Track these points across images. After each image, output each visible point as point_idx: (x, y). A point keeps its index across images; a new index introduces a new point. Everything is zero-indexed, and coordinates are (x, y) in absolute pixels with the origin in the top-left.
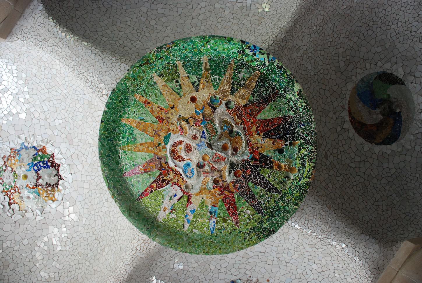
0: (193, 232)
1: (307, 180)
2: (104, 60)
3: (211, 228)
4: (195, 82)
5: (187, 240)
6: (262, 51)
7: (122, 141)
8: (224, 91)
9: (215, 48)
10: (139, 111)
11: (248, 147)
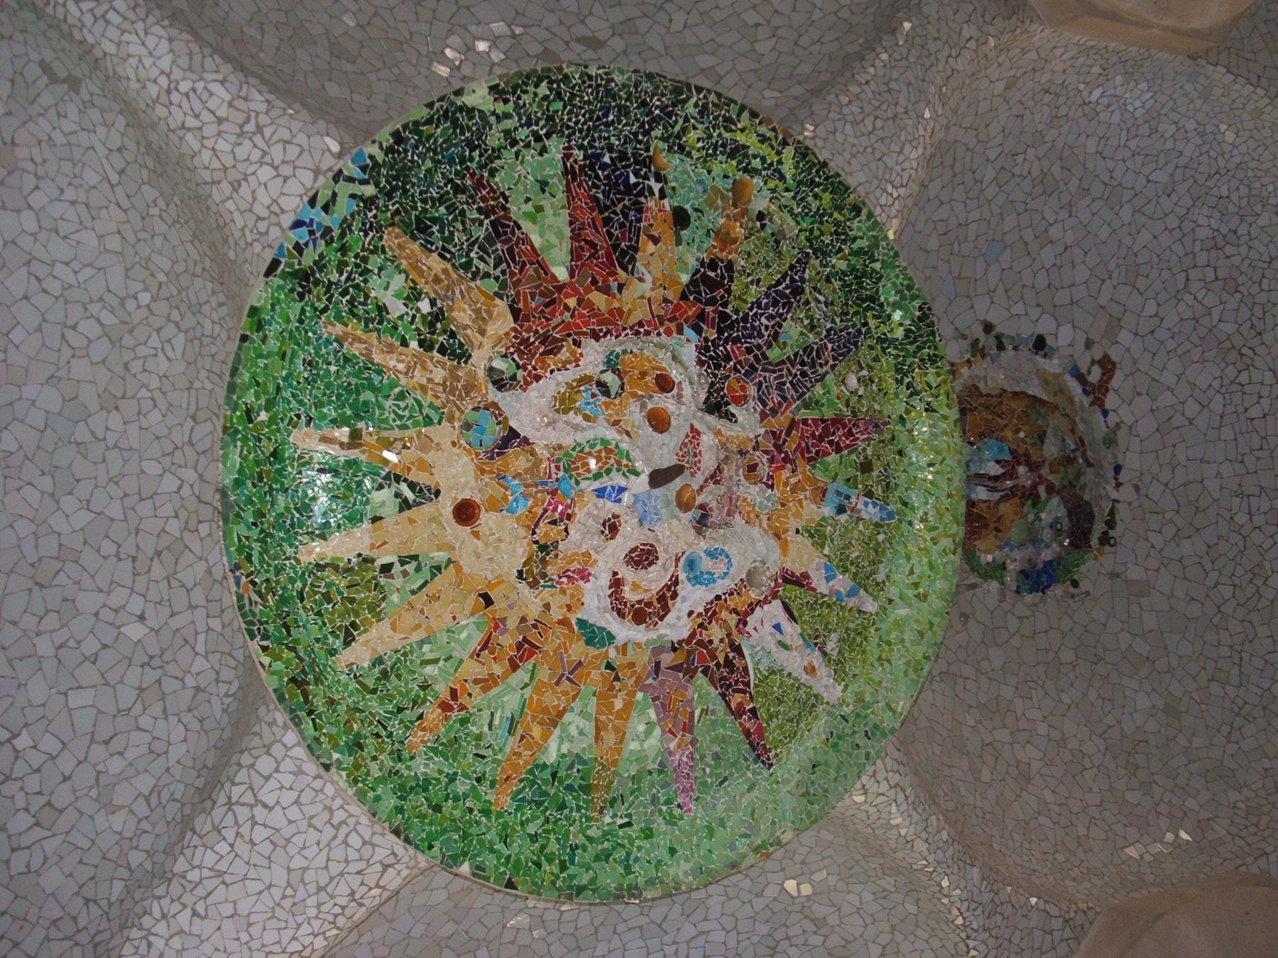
0: (884, 582)
1: (789, 152)
2: (228, 878)
3: (882, 519)
4: (397, 495)
5: (910, 605)
6: (321, 201)
7: (571, 811)
8: (449, 387)
10: (479, 737)
11: (659, 334)
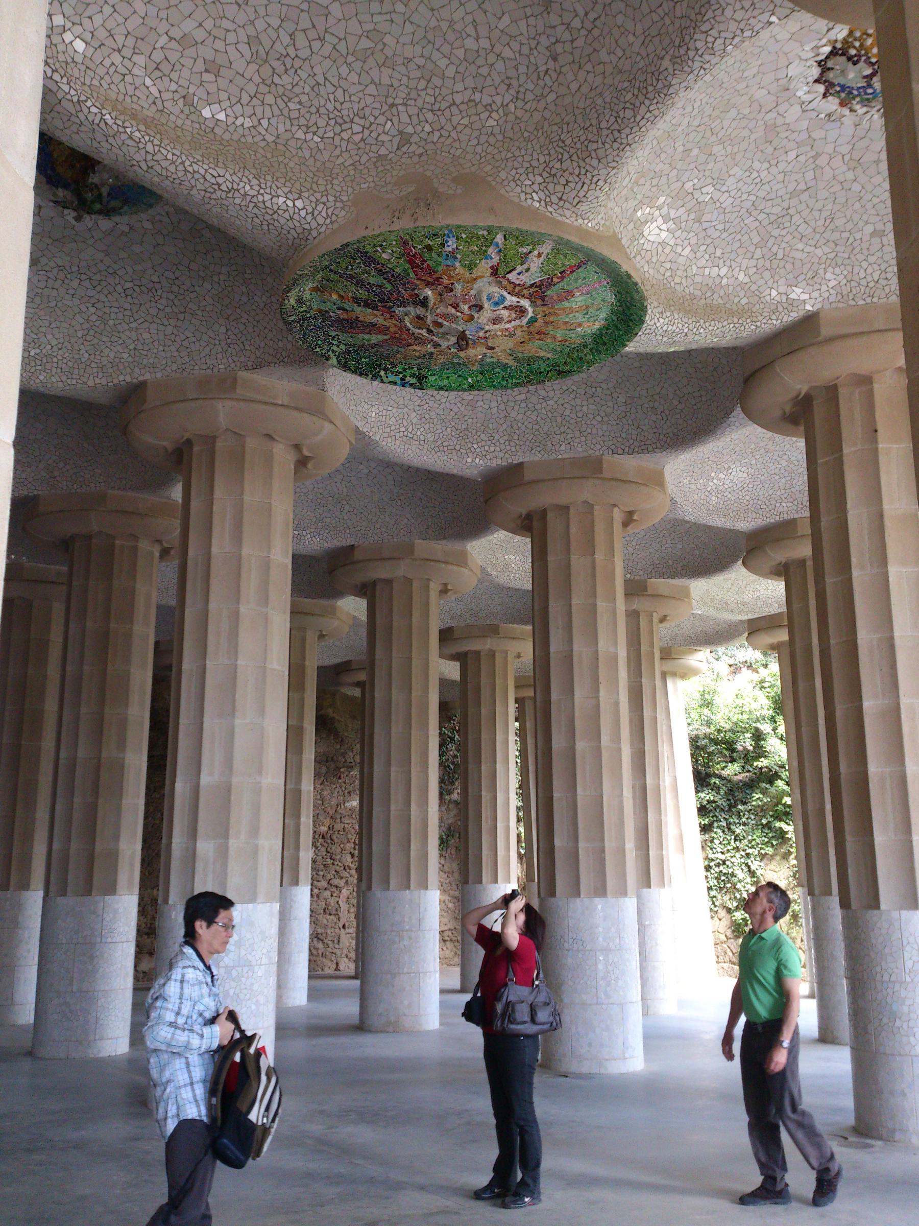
9: (460, 379)
